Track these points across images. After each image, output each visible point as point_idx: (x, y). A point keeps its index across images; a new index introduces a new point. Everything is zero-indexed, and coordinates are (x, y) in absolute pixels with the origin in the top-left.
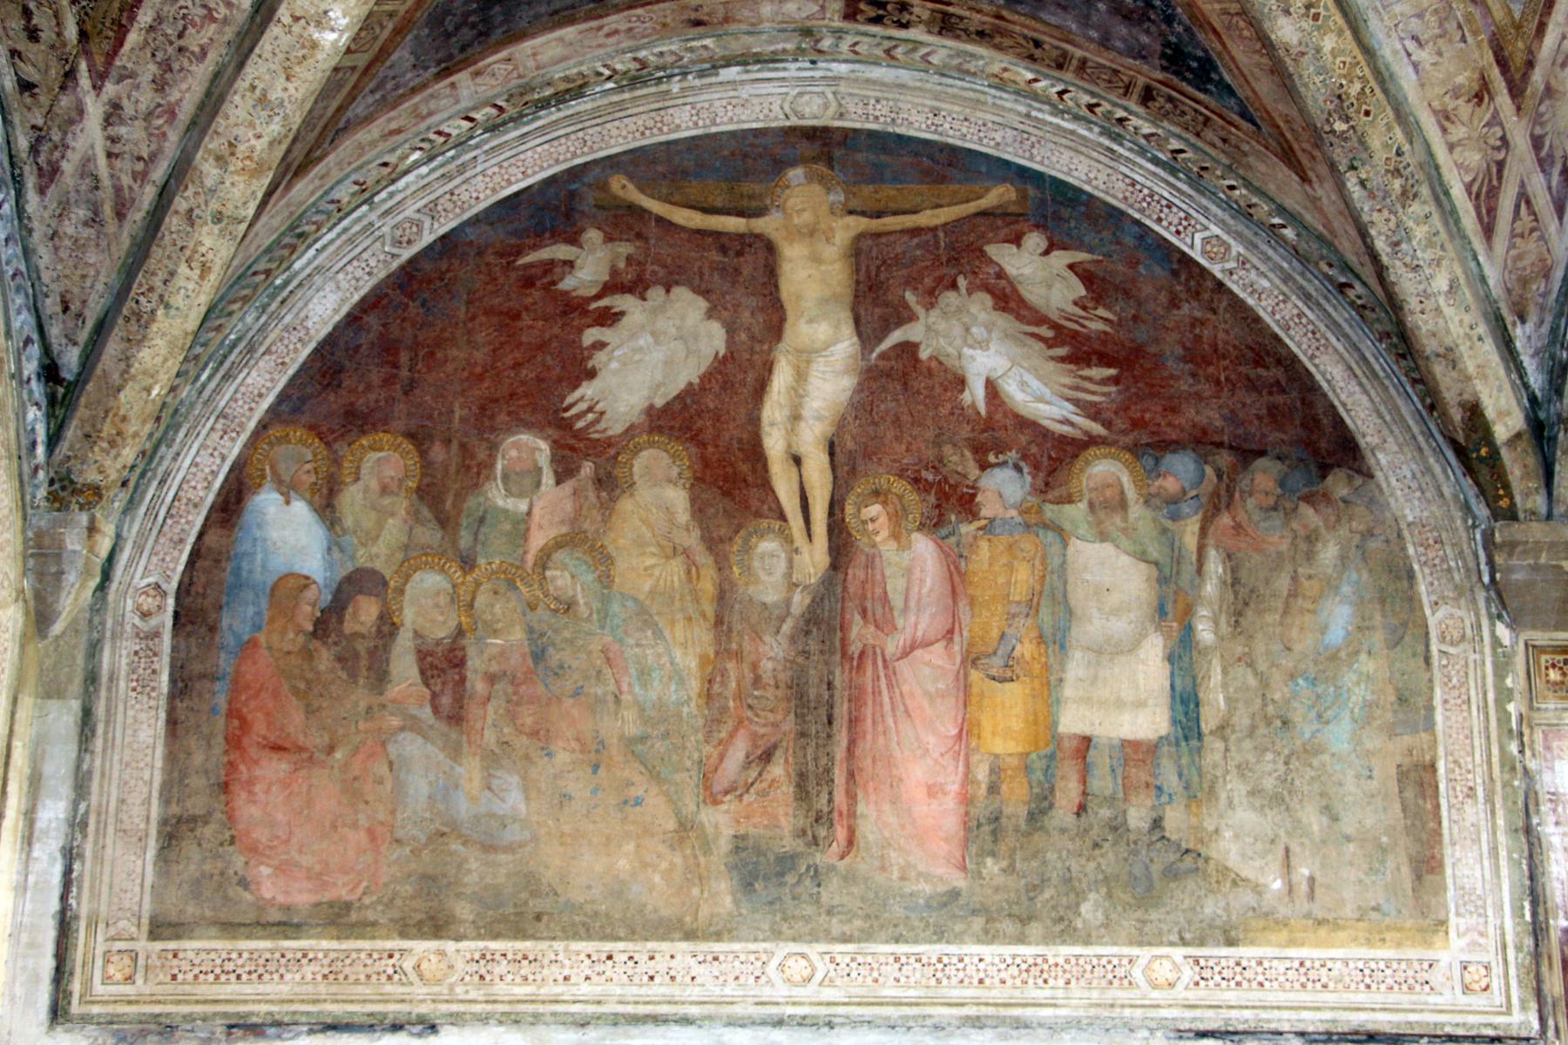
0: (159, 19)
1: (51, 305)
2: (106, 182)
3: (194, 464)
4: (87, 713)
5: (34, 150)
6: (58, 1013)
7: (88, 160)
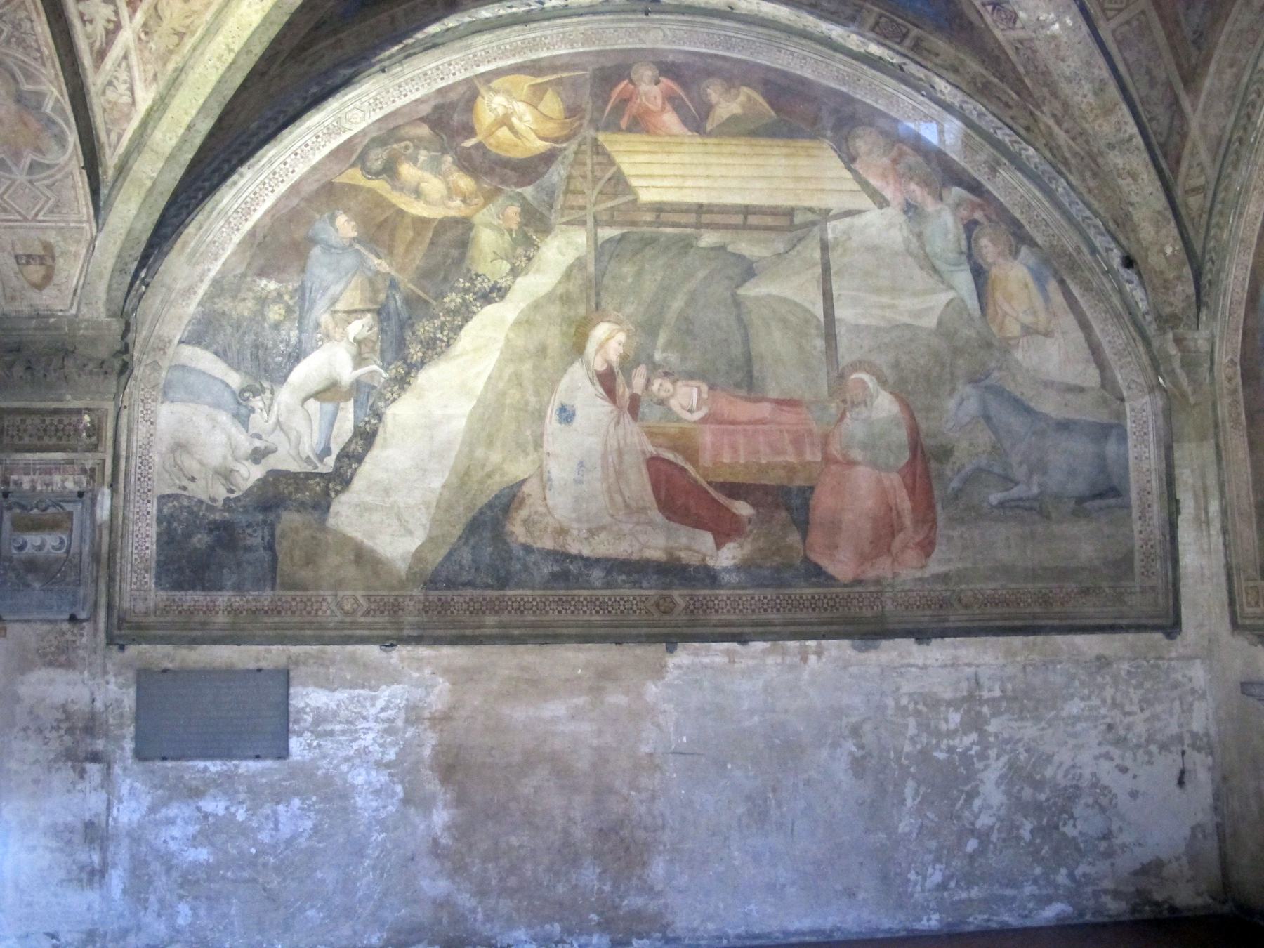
0: (1025, 67)
1: (1112, 226)
2: (1082, 153)
3: (1235, 277)
4: (1217, 446)
5: (1054, 155)
6: (1235, 626)
7: (1070, 148)
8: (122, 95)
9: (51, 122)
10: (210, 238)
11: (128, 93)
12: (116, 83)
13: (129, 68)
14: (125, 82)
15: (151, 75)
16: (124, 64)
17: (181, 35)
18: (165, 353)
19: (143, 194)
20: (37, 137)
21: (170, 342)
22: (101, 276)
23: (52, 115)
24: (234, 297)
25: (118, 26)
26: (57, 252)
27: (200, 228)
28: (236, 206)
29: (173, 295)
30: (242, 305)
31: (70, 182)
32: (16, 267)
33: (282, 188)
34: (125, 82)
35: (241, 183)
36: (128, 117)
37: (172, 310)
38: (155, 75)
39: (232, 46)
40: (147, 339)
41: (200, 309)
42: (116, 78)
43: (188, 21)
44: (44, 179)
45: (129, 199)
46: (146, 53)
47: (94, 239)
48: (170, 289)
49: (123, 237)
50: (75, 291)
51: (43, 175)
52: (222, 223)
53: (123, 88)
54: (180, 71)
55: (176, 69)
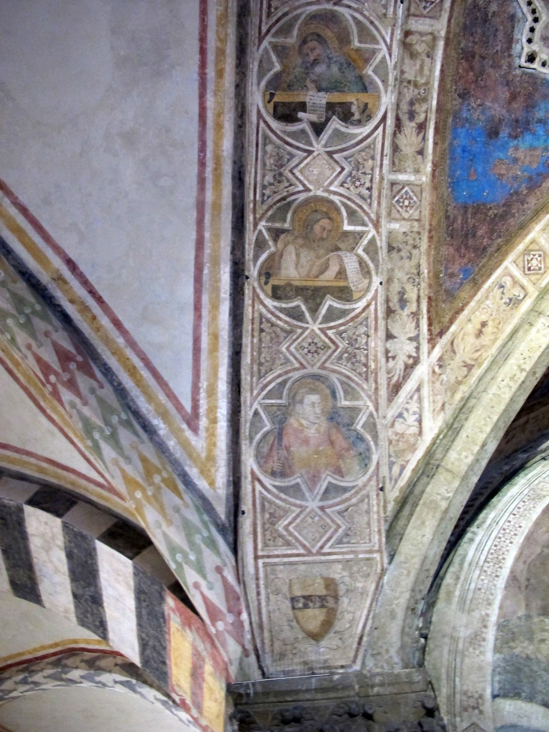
8: (410, 426)
9: (360, 438)
10: (473, 586)
11: (416, 424)
12: (405, 415)
13: (420, 400)
14: (415, 413)
15: (440, 405)
16: (416, 397)
17: (470, 367)
18: (481, 712)
19: (438, 515)
20: (340, 456)
21: (481, 697)
22: (393, 615)
23: (362, 431)
24: (531, 640)
25: (416, 361)
26: (342, 589)
27: (458, 578)
28: (483, 558)
29: (461, 645)
30: (542, 646)
31: (364, 507)
32: (290, 612)
33: (520, 540)
34: (415, 413)
35: (477, 539)
36: (413, 448)
37: (467, 660)
38: (443, 405)
39: (523, 367)
40: (451, 697)
41: (498, 655)
42: (407, 410)
43: (477, 355)
44: (337, 504)
45: (423, 523)
46: (438, 384)
47: (384, 571)
48: (454, 640)
49: (417, 566)
50: (361, 638)
51: (338, 500)
52: (477, 572)
53: (411, 419)
54: (466, 400)
55: (462, 399)
